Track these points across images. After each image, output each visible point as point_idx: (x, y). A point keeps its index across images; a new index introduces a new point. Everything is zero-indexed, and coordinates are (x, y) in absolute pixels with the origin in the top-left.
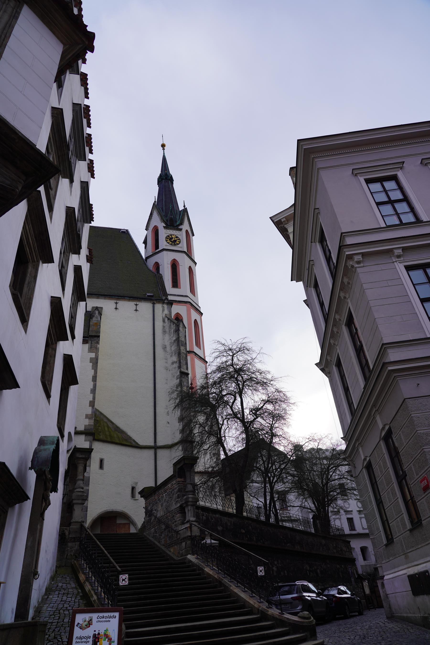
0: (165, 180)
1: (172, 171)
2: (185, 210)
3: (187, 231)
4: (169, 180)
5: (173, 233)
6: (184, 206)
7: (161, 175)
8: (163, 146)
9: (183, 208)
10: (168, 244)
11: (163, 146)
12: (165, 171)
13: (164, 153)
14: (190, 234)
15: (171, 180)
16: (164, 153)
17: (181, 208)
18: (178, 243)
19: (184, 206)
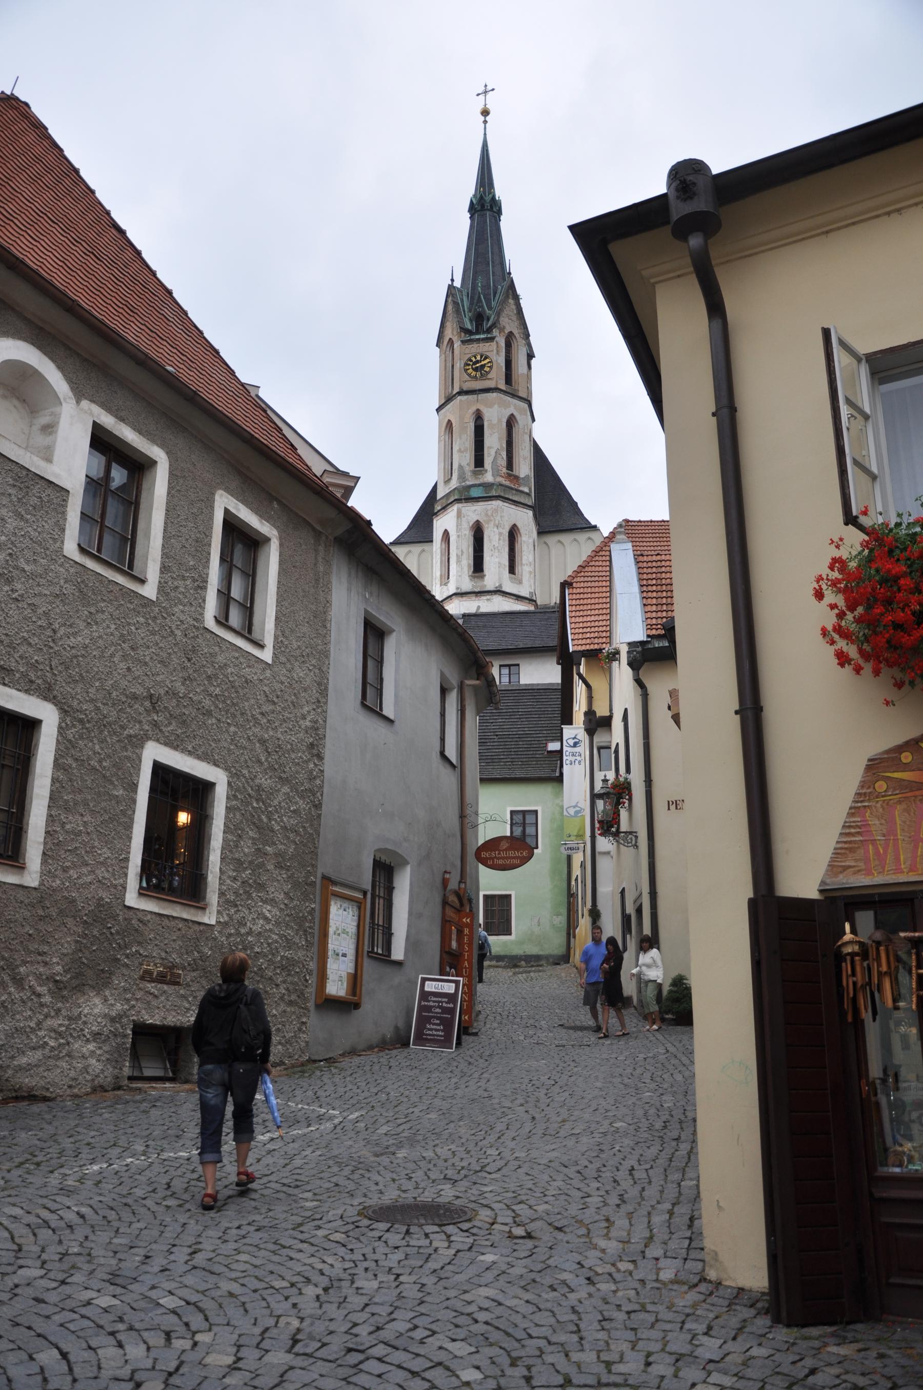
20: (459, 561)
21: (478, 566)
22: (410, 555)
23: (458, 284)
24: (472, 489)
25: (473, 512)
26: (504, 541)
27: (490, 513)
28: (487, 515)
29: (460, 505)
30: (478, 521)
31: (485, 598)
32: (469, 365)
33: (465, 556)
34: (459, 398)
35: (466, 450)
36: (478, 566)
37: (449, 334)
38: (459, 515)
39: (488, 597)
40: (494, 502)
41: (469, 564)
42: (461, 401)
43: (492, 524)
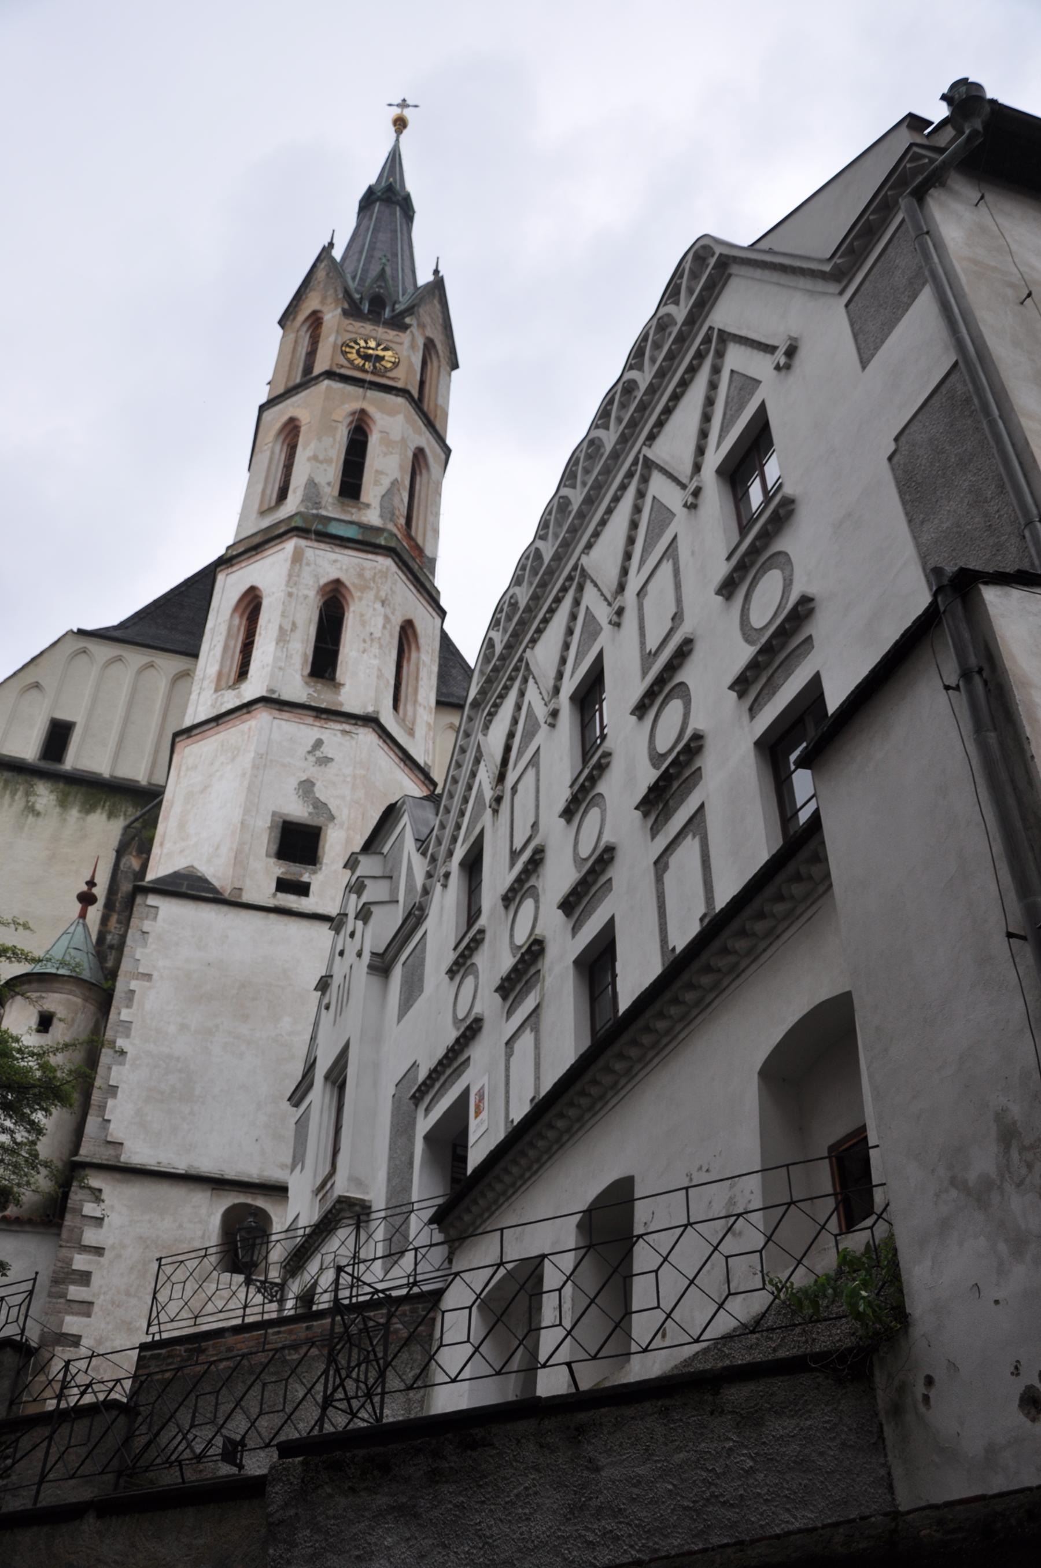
0: (387, 202)
1: (413, 184)
2: (438, 285)
3: (429, 345)
4: (398, 203)
5: (374, 334)
6: (436, 272)
7: (370, 191)
8: (400, 124)
9: (430, 278)
10: (345, 363)
11: (400, 124)
12: (388, 178)
13: (397, 140)
14: (441, 353)
15: (406, 207)
16: (397, 140)
17: (424, 277)
18: (389, 365)
19: (436, 272)
20: (283, 637)
21: (324, 663)
22: (118, 666)
23: (338, 253)
24: (334, 523)
25: (332, 563)
26: (391, 635)
27: (368, 574)
28: (361, 576)
29: (303, 543)
30: (338, 582)
31: (338, 726)
32: (352, 348)
33: (298, 635)
34: (326, 382)
35: (328, 461)
36: (324, 663)
37: (312, 303)
38: (297, 557)
39: (347, 727)
40: (380, 559)
41: (166, 818)
42: (328, 388)
43: (370, 595)
